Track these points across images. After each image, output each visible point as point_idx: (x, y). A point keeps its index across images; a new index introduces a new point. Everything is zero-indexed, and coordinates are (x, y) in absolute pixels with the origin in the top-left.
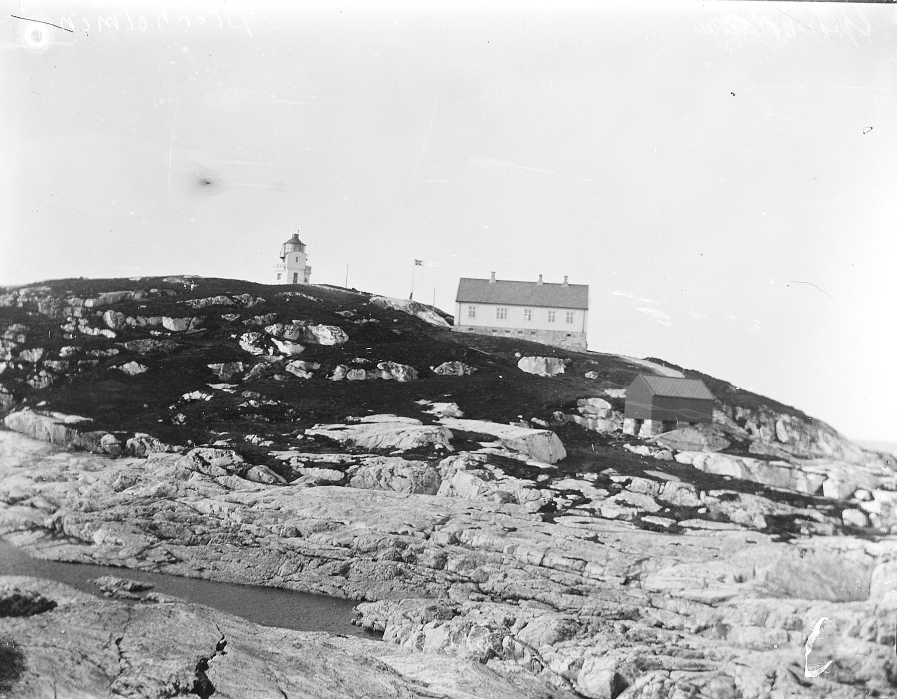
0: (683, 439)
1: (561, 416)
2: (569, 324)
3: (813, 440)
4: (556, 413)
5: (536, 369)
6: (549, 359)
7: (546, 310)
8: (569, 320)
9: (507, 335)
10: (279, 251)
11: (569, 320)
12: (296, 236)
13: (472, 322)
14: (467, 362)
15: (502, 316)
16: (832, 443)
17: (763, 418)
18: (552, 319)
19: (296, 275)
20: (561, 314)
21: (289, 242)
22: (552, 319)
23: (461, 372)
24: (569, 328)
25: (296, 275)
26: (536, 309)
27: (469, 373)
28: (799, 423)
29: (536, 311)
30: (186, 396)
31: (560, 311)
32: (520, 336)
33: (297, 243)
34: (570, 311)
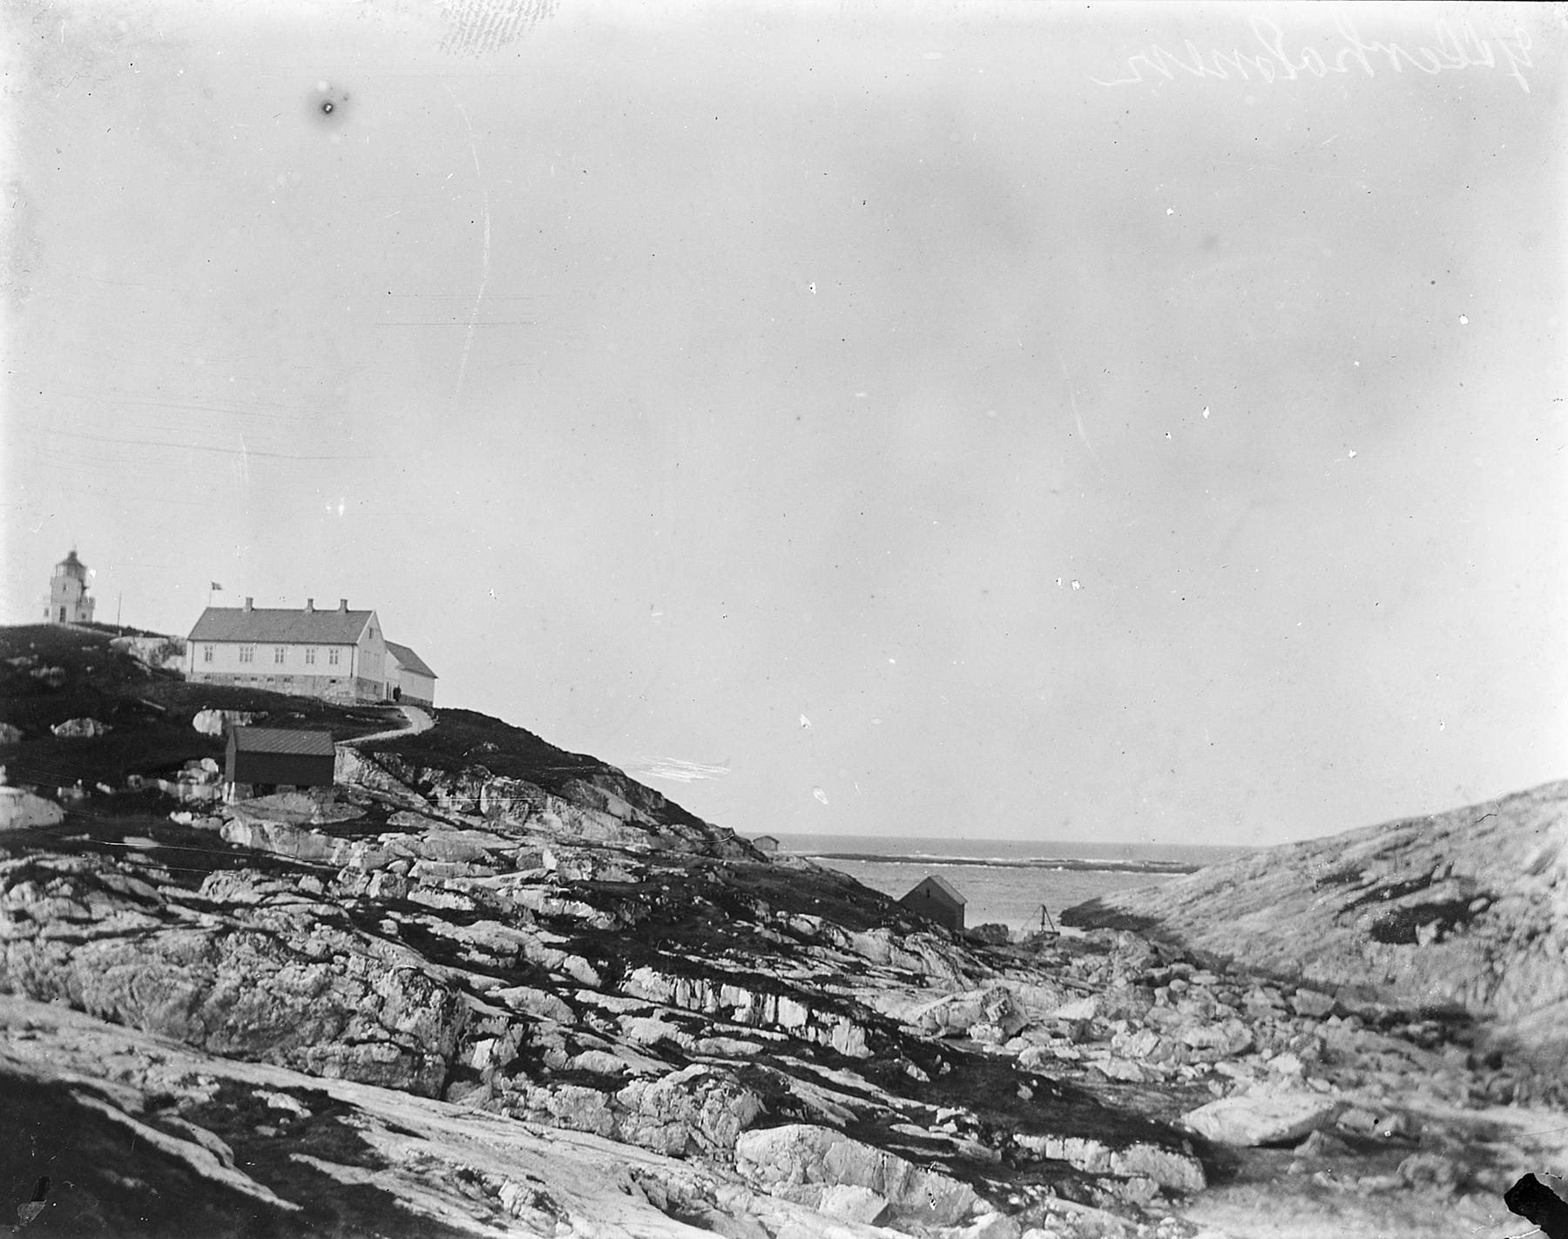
0: (281, 807)
1: (137, 781)
2: (334, 667)
3: (533, 810)
4: (132, 778)
5: (210, 726)
6: (227, 713)
7: (303, 648)
8: (334, 661)
9: (254, 685)
10: (50, 572)
11: (334, 661)
12: (73, 555)
13: (208, 668)
14: (102, 718)
15: (246, 658)
16: (566, 816)
17: (463, 782)
18: (311, 660)
19: (63, 611)
20: (323, 652)
21: (64, 563)
22: (311, 660)
23: (90, 731)
24: (334, 672)
25: (63, 611)
26: (220, 646)
27: (101, 732)
28: (391, 785)
29: (290, 651)
30: (99, 785)
31: (321, 648)
32: (269, 687)
33: (73, 565)
34: (334, 648)
